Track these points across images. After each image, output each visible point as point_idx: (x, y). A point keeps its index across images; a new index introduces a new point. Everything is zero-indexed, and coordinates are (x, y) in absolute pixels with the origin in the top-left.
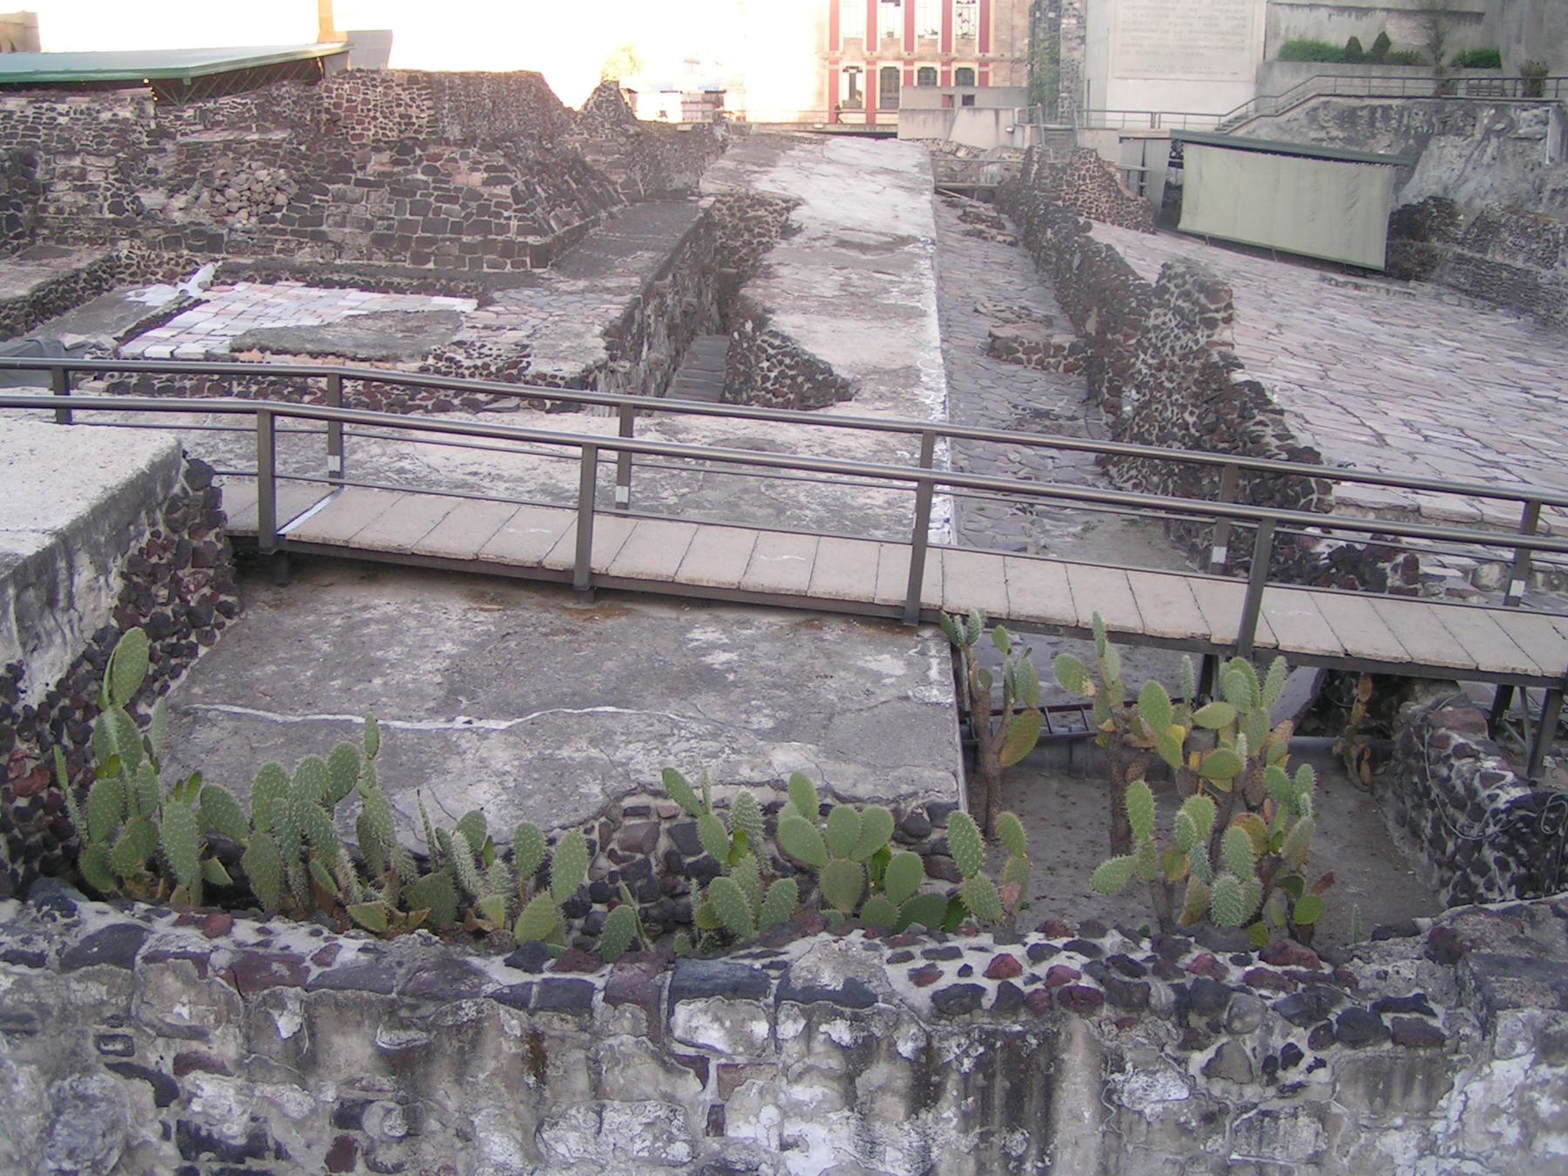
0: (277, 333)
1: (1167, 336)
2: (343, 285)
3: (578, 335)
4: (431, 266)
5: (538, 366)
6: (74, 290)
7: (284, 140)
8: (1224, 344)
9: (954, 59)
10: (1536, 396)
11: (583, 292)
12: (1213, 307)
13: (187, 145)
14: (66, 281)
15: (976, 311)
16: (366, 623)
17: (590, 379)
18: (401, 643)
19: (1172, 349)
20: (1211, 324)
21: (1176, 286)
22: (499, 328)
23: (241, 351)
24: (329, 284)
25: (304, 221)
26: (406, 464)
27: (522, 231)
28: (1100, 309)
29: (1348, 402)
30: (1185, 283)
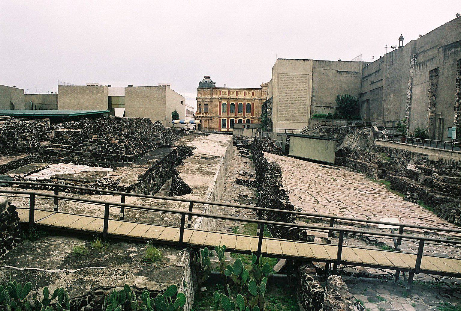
0: (62, 175)
1: (268, 179)
2: (83, 165)
3: (133, 178)
4: (105, 161)
5: (121, 184)
6: (20, 163)
7: (80, 131)
8: (279, 181)
9: (246, 118)
10: (361, 192)
11: (138, 168)
12: (277, 173)
13: (57, 131)
14: (18, 161)
15: (236, 173)
16: (52, 245)
17: (133, 188)
18: (58, 250)
19: (269, 182)
20: (276, 177)
21: (270, 168)
22: (116, 175)
23: (53, 179)
24: (80, 164)
25: (77, 150)
26: (79, 207)
27: (126, 154)
28: (260, 173)
29: (313, 194)
30: (272, 167)
